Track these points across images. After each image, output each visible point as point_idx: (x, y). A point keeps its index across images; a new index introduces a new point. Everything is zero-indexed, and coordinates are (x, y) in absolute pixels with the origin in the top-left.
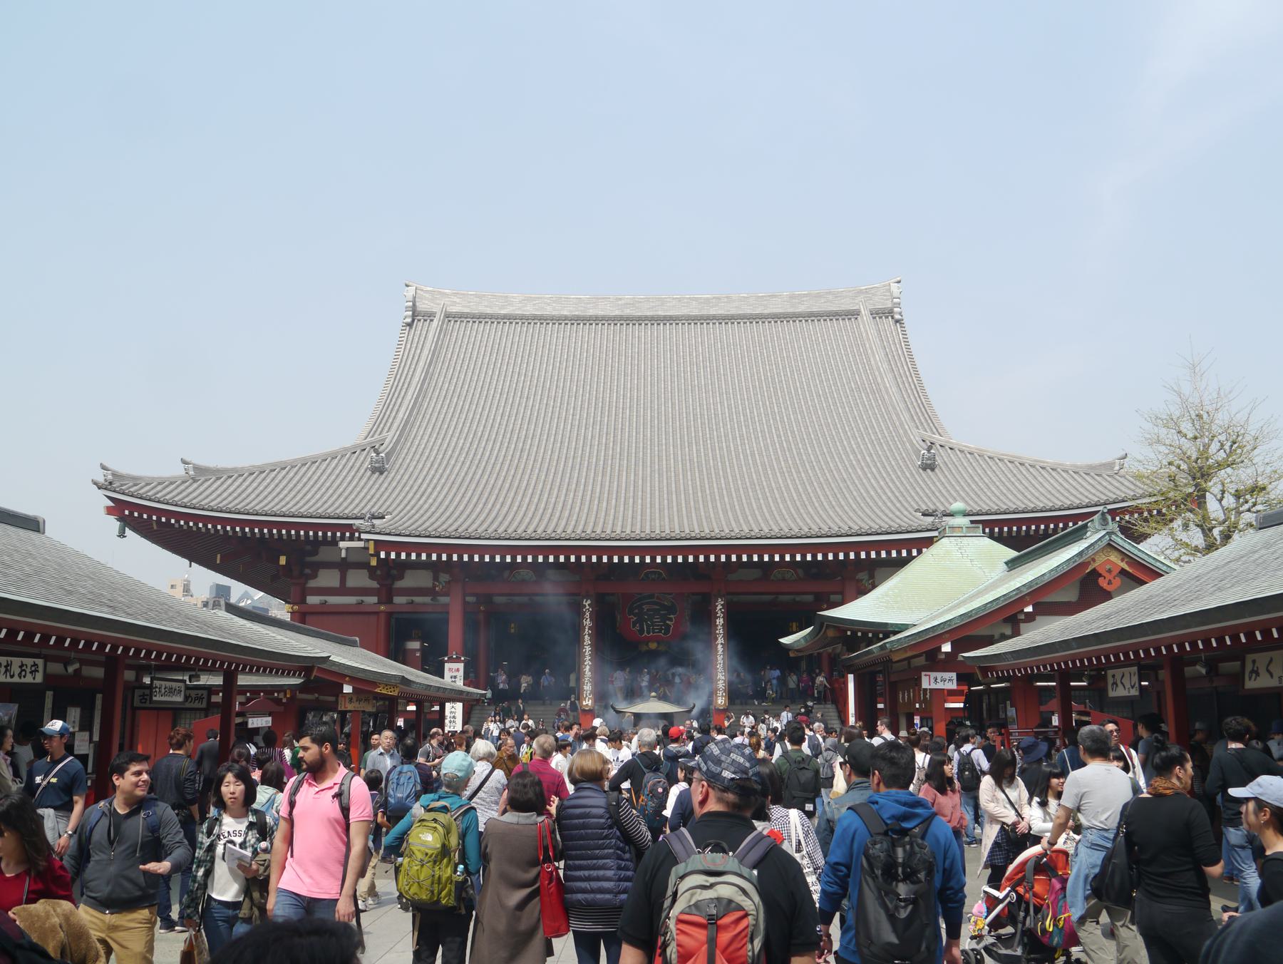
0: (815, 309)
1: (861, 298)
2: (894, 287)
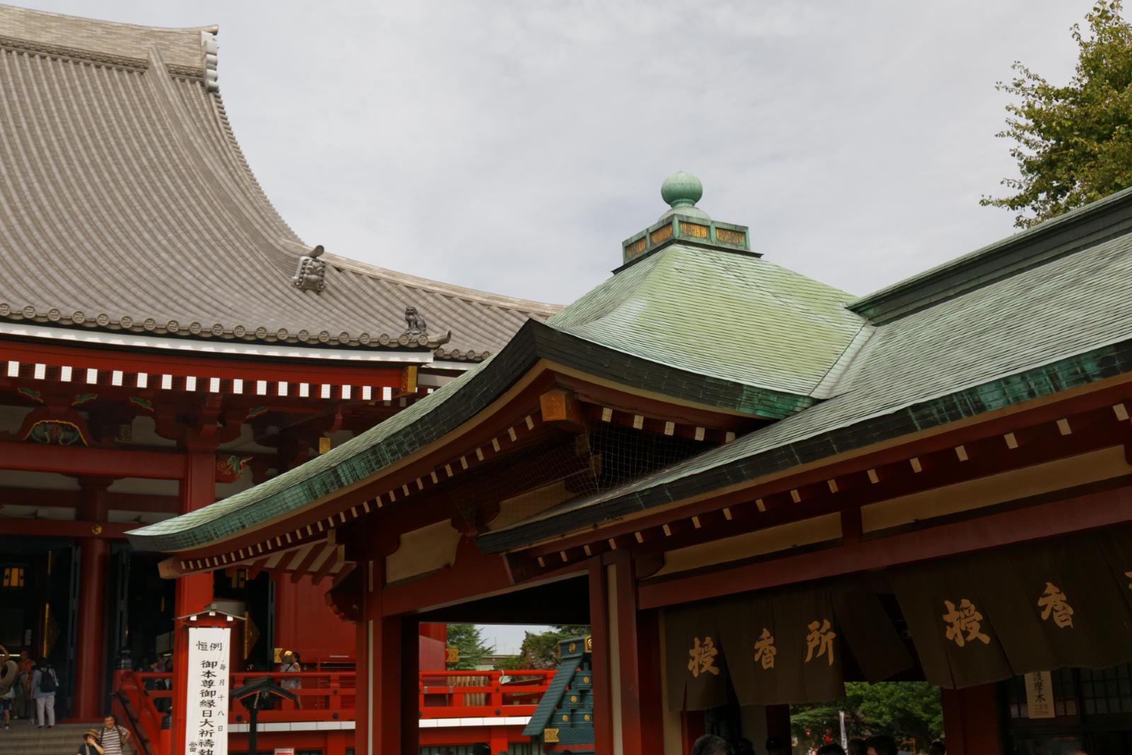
0: (70, 44)
1: (149, 44)
2: (207, 36)
